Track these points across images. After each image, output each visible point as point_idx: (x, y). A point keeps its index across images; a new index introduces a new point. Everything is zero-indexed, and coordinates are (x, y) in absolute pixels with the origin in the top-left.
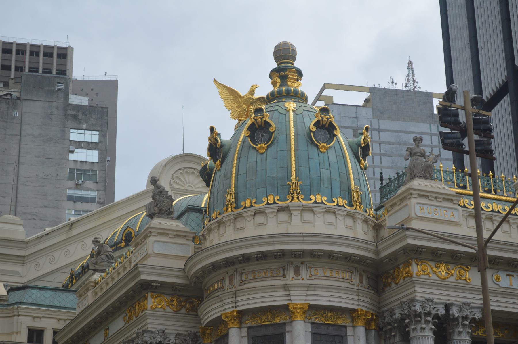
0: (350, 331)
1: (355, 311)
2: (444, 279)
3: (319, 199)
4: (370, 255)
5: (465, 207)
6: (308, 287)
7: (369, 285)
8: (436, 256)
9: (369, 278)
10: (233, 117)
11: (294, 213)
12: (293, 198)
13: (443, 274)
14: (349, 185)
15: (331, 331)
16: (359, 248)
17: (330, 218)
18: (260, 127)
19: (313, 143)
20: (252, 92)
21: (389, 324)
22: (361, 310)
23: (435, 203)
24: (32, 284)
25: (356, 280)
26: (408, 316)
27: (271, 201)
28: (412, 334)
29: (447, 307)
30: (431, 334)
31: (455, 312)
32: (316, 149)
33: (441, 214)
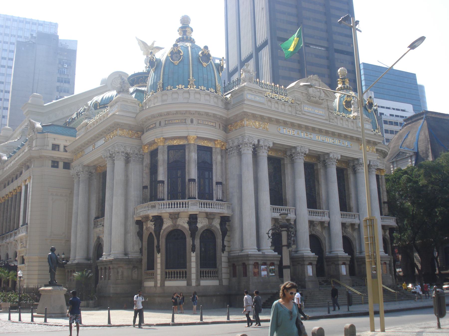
1: (217, 140)
2: (257, 128)
4: (225, 116)
5: (267, 96)
10: (144, 54)
12: (191, 87)
14: (215, 83)
18: (176, 53)
19: (200, 62)
20: (153, 44)
21: (232, 147)
23: (255, 94)
24: (55, 123)
26: (242, 144)
27: (180, 87)
28: (242, 152)
29: (259, 141)
30: (251, 152)
31: (261, 143)
33: (257, 99)
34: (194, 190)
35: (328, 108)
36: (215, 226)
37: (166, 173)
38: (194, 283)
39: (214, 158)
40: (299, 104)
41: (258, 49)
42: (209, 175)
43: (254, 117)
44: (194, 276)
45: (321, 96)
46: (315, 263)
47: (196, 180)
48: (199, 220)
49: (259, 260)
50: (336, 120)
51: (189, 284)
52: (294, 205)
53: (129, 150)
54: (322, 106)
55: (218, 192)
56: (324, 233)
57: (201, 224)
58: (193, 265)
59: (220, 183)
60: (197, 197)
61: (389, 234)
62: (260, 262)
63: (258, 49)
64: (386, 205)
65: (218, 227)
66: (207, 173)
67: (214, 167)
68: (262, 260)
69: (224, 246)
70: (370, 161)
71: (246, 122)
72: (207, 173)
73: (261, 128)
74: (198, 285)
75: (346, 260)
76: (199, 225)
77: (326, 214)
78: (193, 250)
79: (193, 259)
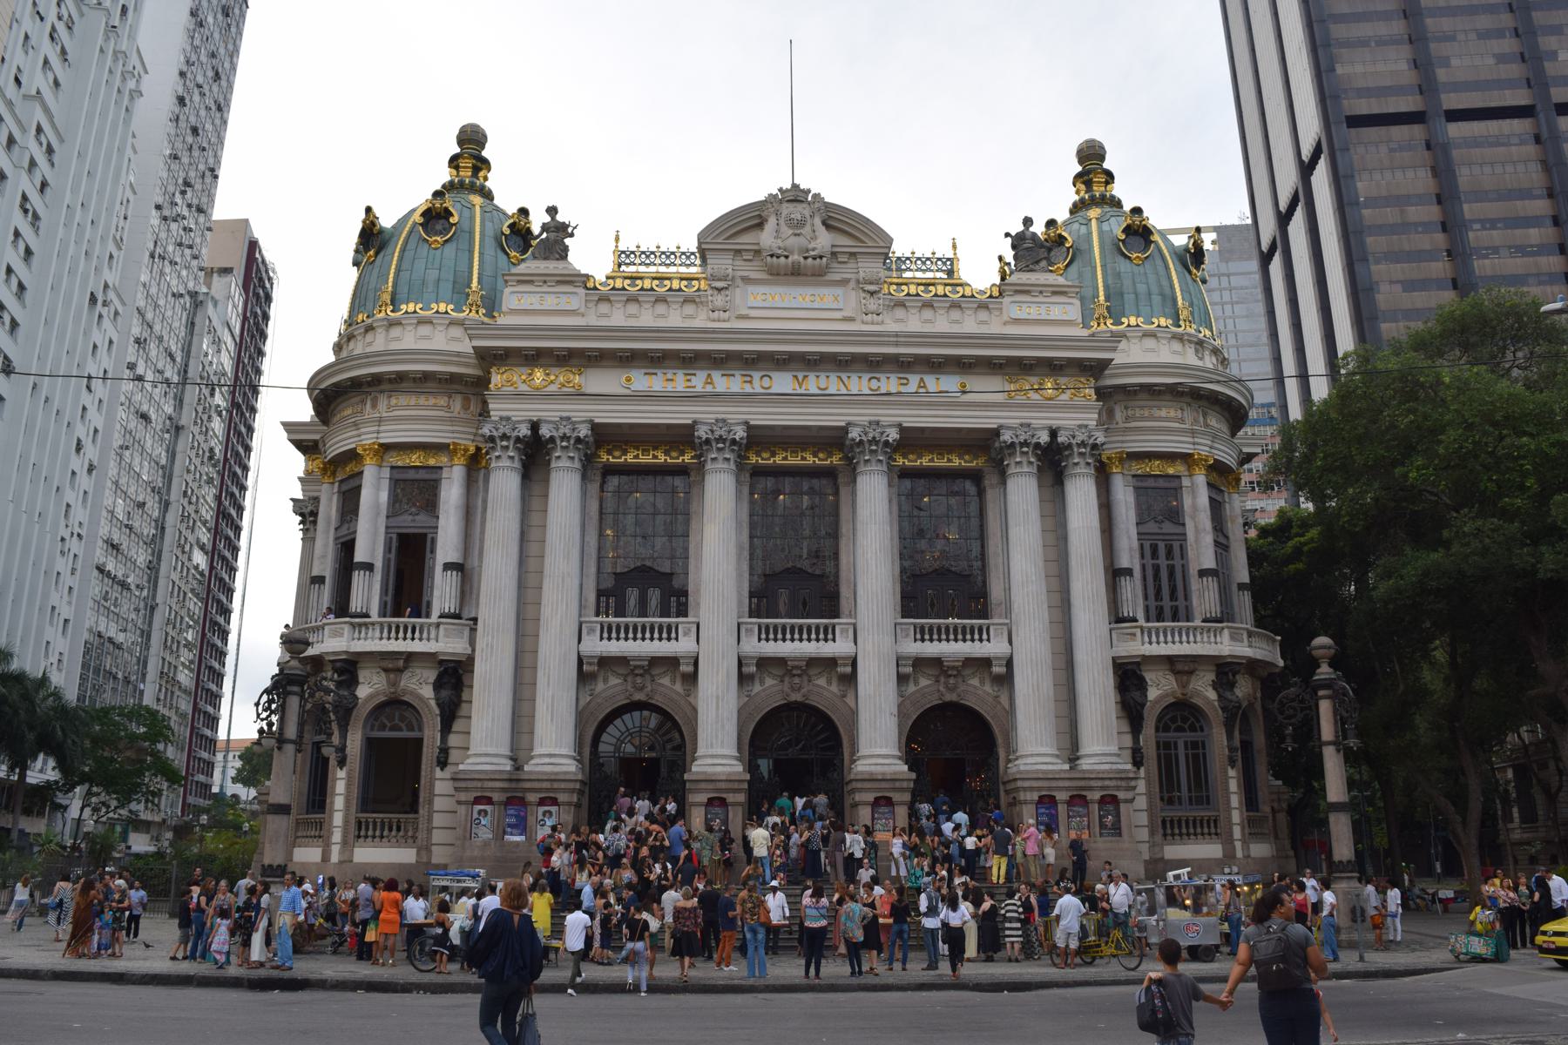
3: (411, 307)
5: (595, 288)
8: (534, 358)
15: (422, 475)
17: (424, 330)
23: (545, 289)
25: (457, 404)
29: (535, 426)
31: (545, 431)
33: (550, 302)
34: (367, 592)
35: (858, 282)
36: (413, 693)
38: (335, 857)
40: (719, 290)
41: (1306, 169)
43: (534, 358)
44: (337, 836)
45: (812, 245)
46: (741, 798)
47: (379, 565)
48: (363, 675)
49: (493, 789)
50: (900, 313)
51: (326, 857)
54: (830, 277)
55: (442, 591)
56: (850, 700)
57: (369, 687)
58: (339, 803)
61: (1215, 686)
62: (496, 797)
63: (1306, 169)
65: (427, 692)
67: (442, 522)
68: (503, 790)
69: (444, 751)
70: (1054, 433)
71: (497, 379)
73: (553, 388)
74: (347, 861)
75: (894, 789)
76: (363, 692)
78: (342, 763)
79: (341, 785)
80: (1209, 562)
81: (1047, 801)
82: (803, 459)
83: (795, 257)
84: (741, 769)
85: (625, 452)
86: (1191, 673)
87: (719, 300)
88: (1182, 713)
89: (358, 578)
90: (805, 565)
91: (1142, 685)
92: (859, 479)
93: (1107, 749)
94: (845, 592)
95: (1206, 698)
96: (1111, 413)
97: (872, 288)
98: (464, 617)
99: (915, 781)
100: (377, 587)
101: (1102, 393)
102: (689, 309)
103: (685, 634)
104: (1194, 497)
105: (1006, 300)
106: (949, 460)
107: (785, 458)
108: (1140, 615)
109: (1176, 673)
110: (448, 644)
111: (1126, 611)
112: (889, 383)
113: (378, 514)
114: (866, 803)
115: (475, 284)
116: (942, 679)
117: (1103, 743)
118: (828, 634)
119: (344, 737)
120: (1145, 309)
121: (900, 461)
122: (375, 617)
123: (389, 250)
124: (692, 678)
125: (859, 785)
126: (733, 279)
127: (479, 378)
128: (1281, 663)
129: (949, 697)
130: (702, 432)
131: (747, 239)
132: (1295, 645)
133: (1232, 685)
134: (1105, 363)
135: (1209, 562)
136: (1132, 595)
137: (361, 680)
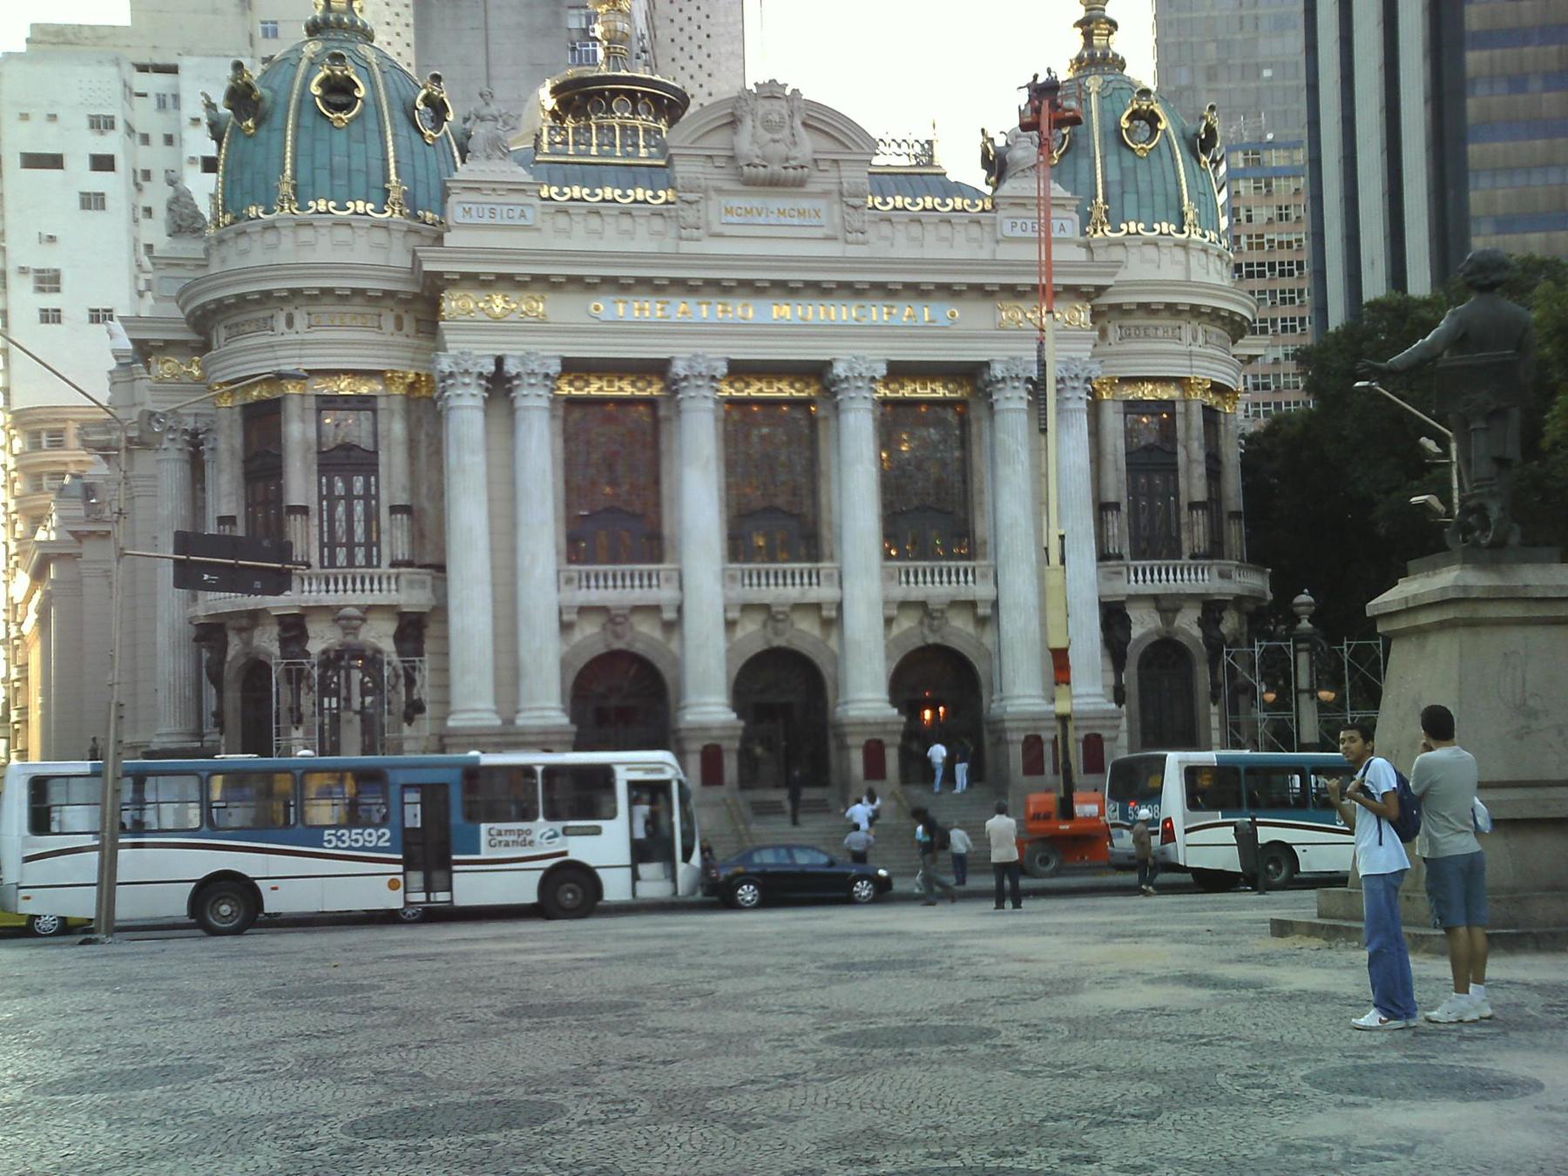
0: (382, 403)
2: (497, 319)
6: (303, 344)
7: (418, 331)
9: (418, 320)
11: (284, 232)
13: (498, 310)
14: (387, 179)
16: (377, 278)
17: (343, 234)
22: (393, 371)
23: (493, 198)
25: (388, 322)
29: (499, 361)
31: (511, 367)
32: (327, 125)
35: (841, 194)
37: (242, 492)
39: (380, 427)
42: (367, 485)
45: (793, 153)
47: (314, 507)
50: (885, 229)
52: (679, 560)
53: (190, 424)
54: (810, 188)
59: (406, 509)
60: (315, 559)
61: (1200, 623)
64: (1200, 516)
65: (388, 646)
66: (358, 483)
71: (454, 304)
72: (358, 483)
76: (315, 647)
77: (830, 576)
80: (1200, 494)
81: (1033, 744)
82: (780, 390)
83: (776, 168)
84: (734, 716)
85: (588, 384)
86: (1177, 610)
87: (690, 215)
88: (1166, 651)
89: (295, 527)
90: (780, 502)
91: (1126, 623)
92: (843, 417)
93: (1091, 690)
94: (825, 532)
95: (1191, 636)
96: (1103, 334)
97: (857, 202)
98: (433, 563)
99: (906, 725)
100: (315, 531)
101: (1096, 315)
102: (658, 223)
103: (668, 580)
104: (1188, 428)
105: (1001, 214)
106: (934, 391)
107: (760, 390)
108: (1126, 550)
109: (1161, 611)
110: (412, 596)
111: (1112, 548)
112: (877, 312)
113: (309, 449)
114: (857, 747)
115: (393, 177)
116: (926, 621)
117: (1090, 690)
118: (815, 577)
119: (297, 695)
120: (1146, 212)
121: (883, 392)
122: (316, 569)
123: (277, 121)
124: (673, 626)
125: (851, 729)
126: (706, 191)
127: (415, 294)
128: (1270, 597)
129: (931, 640)
130: (679, 368)
131: (718, 142)
132: (1284, 587)
133: (1218, 621)
134: (1100, 290)
135: (1200, 494)
136: (1118, 526)
137: (311, 633)
